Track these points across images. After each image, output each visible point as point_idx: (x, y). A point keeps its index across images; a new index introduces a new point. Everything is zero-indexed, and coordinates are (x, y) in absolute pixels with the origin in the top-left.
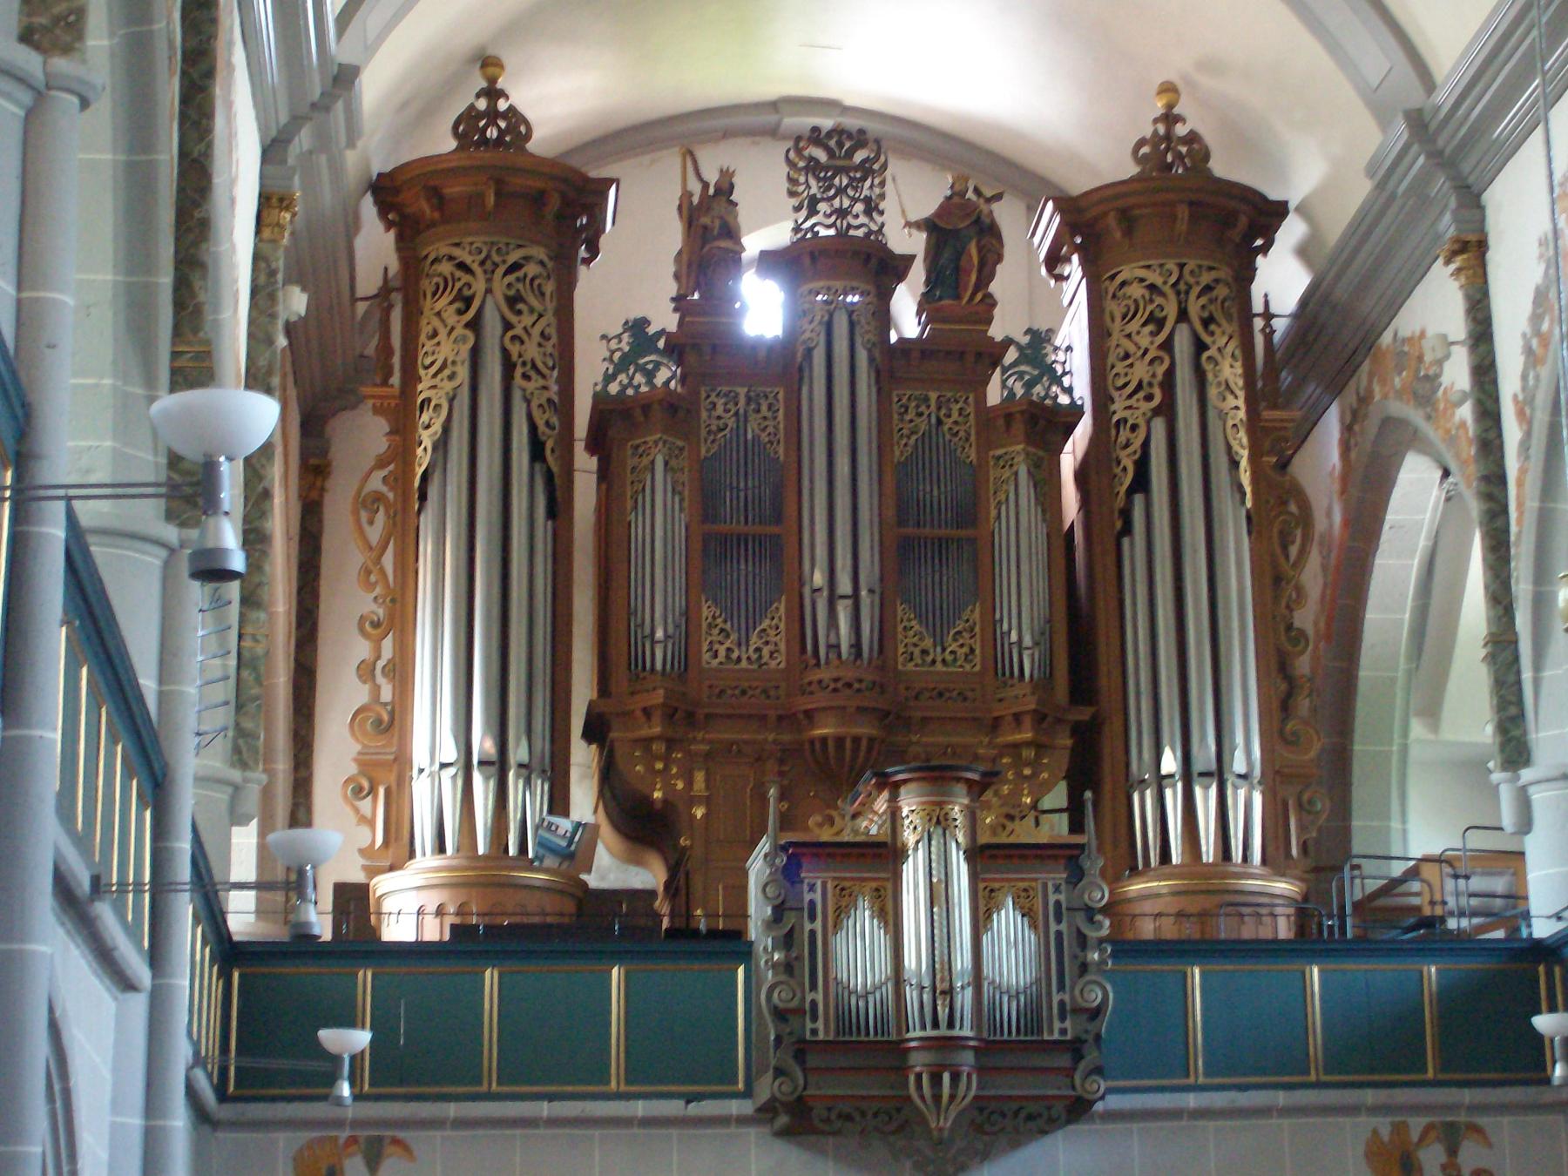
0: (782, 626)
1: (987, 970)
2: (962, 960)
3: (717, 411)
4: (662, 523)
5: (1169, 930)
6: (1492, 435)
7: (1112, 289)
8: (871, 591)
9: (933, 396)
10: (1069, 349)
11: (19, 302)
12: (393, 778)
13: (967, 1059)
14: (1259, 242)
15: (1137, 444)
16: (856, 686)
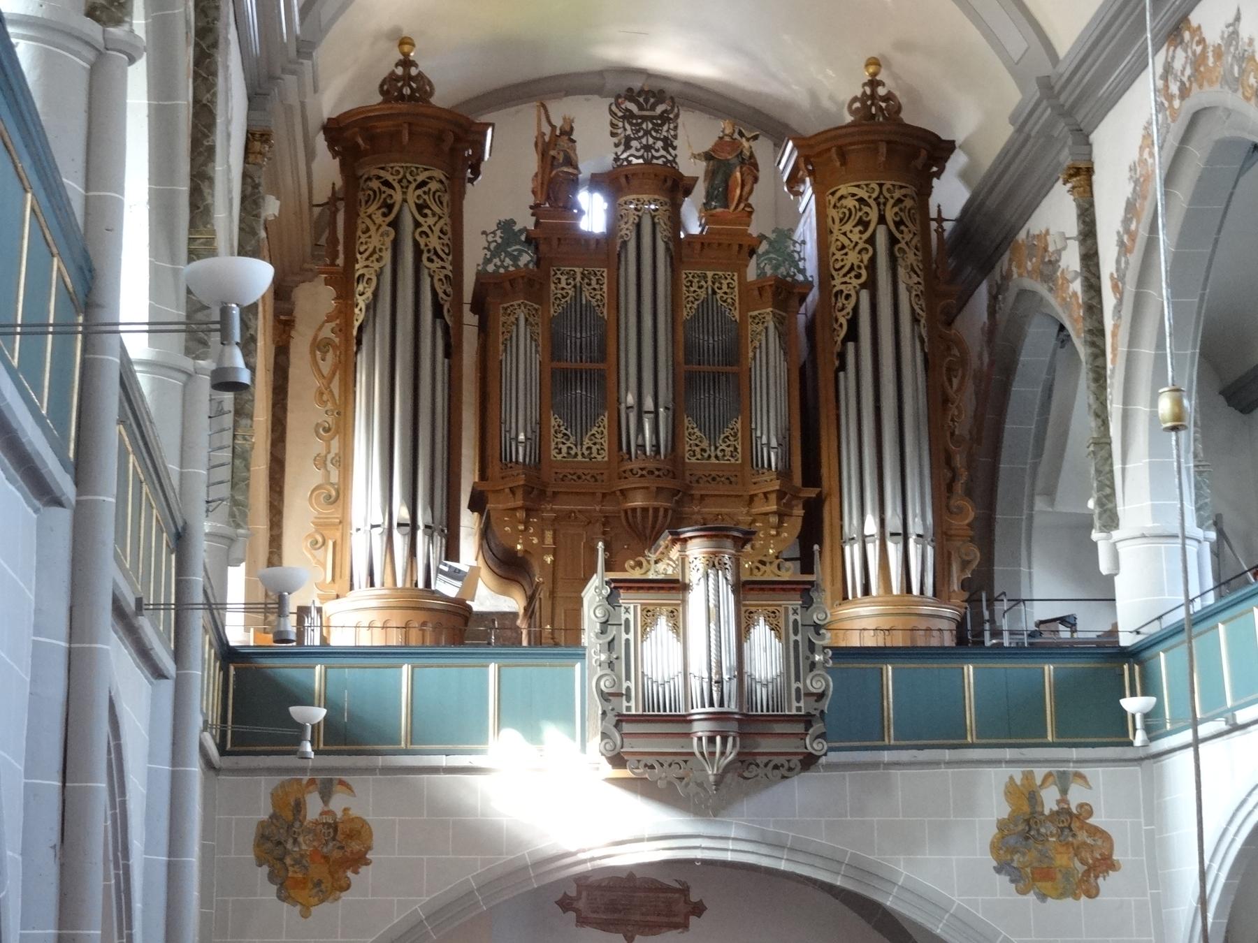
0: (606, 432)
1: (747, 668)
2: (729, 660)
3: (561, 285)
4: (523, 361)
5: (870, 641)
6: (1094, 302)
7: (833, 200)
8: (667, 408)
9: (710, 274)
10: (804, 242)
11: (87, 199)
12: (338, 535)
13: (733, 727)
14: (935, 169)
15: (849, 309)
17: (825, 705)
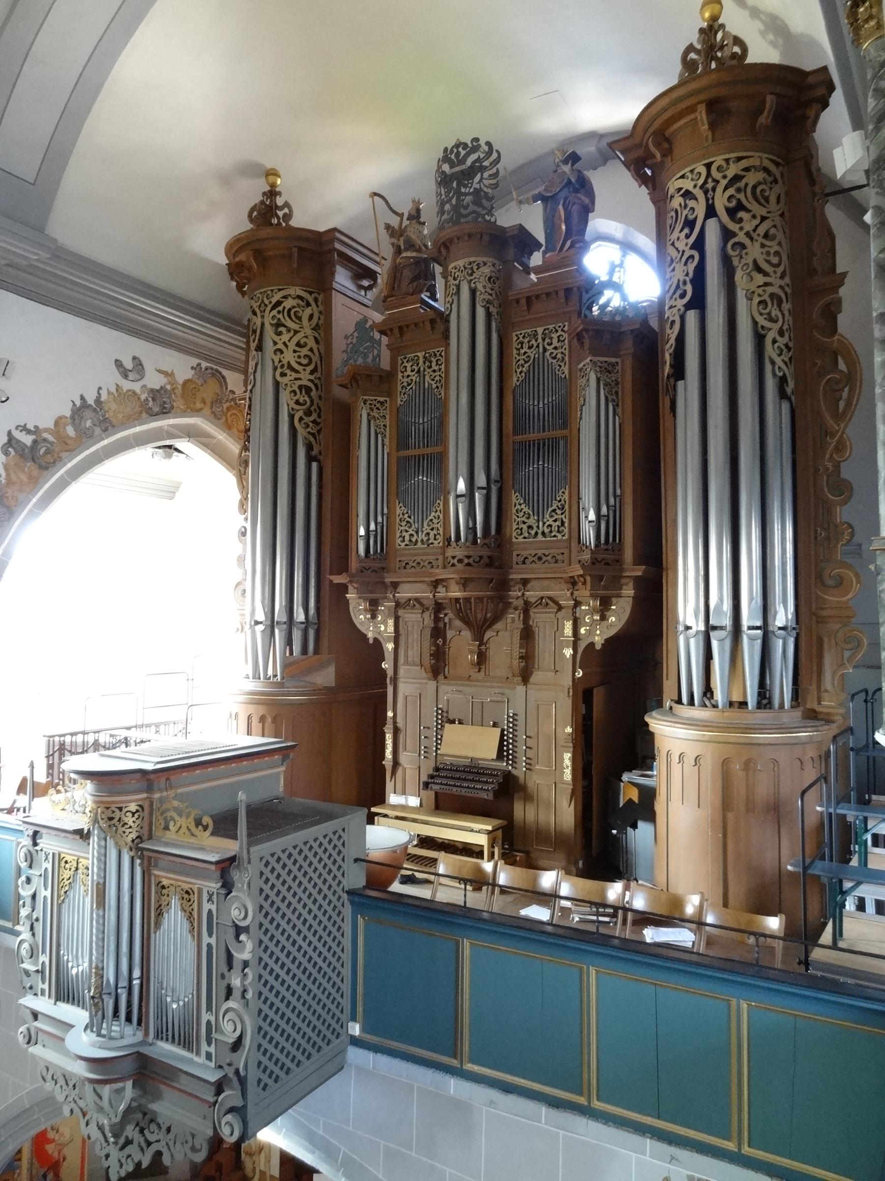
0: (441, 516)
9: (540, 330)
16: (466, 561)
17: (241, 1059)
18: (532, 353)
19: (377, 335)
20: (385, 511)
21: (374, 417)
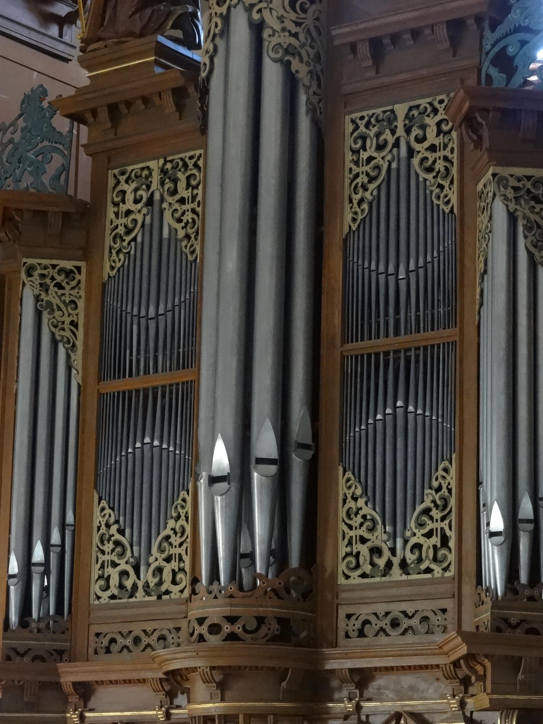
9: (401, 109)
16: (227, 628)
18: (382, 159)
19: (61, 123)
20: (70, 518)
21: (49, 304)
